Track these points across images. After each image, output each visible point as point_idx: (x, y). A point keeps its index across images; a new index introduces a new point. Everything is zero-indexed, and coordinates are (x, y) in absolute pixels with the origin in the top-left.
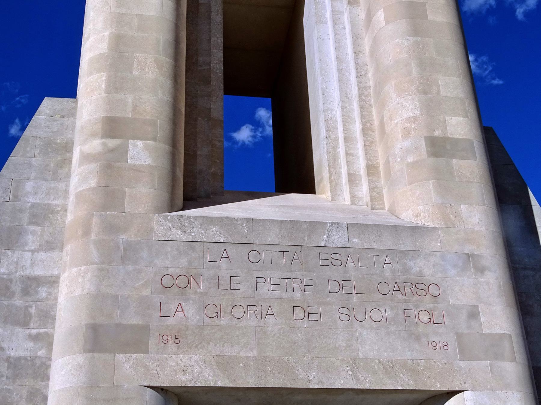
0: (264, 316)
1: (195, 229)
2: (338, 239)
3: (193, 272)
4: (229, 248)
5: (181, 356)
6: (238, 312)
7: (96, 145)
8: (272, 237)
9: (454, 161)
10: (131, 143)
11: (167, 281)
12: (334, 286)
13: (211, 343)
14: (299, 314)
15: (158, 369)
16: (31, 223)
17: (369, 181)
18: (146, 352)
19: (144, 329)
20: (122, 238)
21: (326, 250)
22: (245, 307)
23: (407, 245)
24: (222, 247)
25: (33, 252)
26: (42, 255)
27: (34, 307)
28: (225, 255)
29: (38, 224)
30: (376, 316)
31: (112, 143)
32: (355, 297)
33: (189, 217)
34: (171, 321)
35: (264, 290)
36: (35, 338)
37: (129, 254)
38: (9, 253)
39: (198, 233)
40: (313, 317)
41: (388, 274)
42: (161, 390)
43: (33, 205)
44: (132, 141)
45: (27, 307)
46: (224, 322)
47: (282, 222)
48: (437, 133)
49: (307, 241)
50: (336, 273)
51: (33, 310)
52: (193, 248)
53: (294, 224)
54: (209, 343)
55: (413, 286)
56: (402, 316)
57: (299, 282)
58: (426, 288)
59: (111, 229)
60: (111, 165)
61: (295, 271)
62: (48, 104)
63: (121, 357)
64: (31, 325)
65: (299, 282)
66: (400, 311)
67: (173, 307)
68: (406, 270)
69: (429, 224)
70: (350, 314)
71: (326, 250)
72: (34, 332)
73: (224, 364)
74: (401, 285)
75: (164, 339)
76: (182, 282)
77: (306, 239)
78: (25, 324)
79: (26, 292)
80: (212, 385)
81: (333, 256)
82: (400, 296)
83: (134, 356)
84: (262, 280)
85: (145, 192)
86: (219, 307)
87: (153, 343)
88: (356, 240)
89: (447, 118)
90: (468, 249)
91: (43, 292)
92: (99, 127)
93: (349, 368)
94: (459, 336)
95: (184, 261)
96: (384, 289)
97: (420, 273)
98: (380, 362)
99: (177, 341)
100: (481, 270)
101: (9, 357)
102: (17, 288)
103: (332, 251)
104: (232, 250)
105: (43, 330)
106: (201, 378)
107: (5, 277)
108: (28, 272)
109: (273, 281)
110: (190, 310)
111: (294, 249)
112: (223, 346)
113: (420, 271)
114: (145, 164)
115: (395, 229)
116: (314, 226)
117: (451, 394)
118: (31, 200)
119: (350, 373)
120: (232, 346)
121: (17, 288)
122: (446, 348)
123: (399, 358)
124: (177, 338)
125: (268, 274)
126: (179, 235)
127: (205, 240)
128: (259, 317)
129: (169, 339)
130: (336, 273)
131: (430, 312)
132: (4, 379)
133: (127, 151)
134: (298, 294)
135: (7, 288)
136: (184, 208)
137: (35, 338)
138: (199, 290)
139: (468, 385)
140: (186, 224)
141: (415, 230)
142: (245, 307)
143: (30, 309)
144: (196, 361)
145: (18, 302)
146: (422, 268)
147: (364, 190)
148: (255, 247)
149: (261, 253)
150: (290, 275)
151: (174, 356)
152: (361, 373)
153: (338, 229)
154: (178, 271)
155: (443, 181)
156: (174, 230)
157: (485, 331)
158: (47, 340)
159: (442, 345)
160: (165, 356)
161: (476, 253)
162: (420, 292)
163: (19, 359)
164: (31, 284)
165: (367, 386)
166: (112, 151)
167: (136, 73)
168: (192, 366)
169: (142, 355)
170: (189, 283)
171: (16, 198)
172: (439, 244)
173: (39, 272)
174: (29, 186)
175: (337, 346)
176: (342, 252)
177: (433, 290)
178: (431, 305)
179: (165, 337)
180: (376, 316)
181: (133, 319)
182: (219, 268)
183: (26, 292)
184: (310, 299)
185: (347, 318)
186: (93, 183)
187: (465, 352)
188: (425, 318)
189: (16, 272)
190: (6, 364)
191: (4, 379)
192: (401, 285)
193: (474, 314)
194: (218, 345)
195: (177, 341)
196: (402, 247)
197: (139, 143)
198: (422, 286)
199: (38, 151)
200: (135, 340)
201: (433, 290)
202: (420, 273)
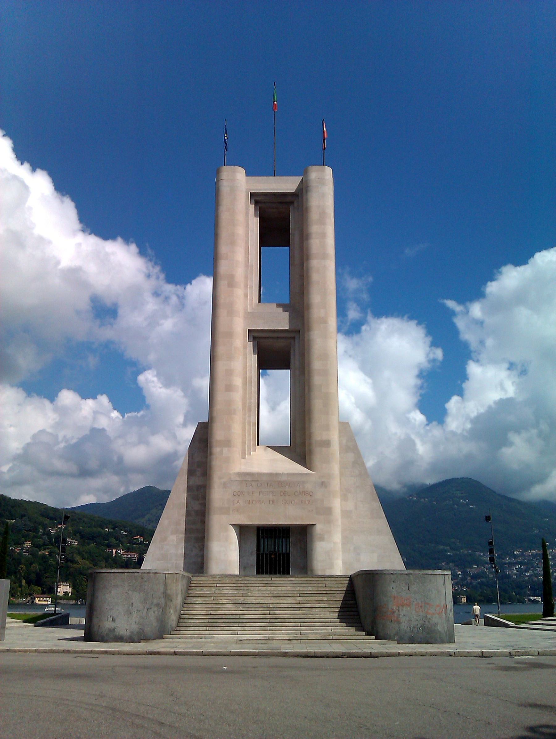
2: (284, 478)
12: (282, 494)
35: (261, 495)
46: (250, 505)
55: (304, 493)
76: (239, 493)
79: (197, 490)
82: (300, 496)
90: (323, 480)
104: (253, 483)
116: (277, 474)
124: (237, 510)
126: (238, 479)
134: (271, 496)
146: (309, 487)
177: (311, 494)
181: (226, 506)
188: (307, 502)
200: (225, 511)
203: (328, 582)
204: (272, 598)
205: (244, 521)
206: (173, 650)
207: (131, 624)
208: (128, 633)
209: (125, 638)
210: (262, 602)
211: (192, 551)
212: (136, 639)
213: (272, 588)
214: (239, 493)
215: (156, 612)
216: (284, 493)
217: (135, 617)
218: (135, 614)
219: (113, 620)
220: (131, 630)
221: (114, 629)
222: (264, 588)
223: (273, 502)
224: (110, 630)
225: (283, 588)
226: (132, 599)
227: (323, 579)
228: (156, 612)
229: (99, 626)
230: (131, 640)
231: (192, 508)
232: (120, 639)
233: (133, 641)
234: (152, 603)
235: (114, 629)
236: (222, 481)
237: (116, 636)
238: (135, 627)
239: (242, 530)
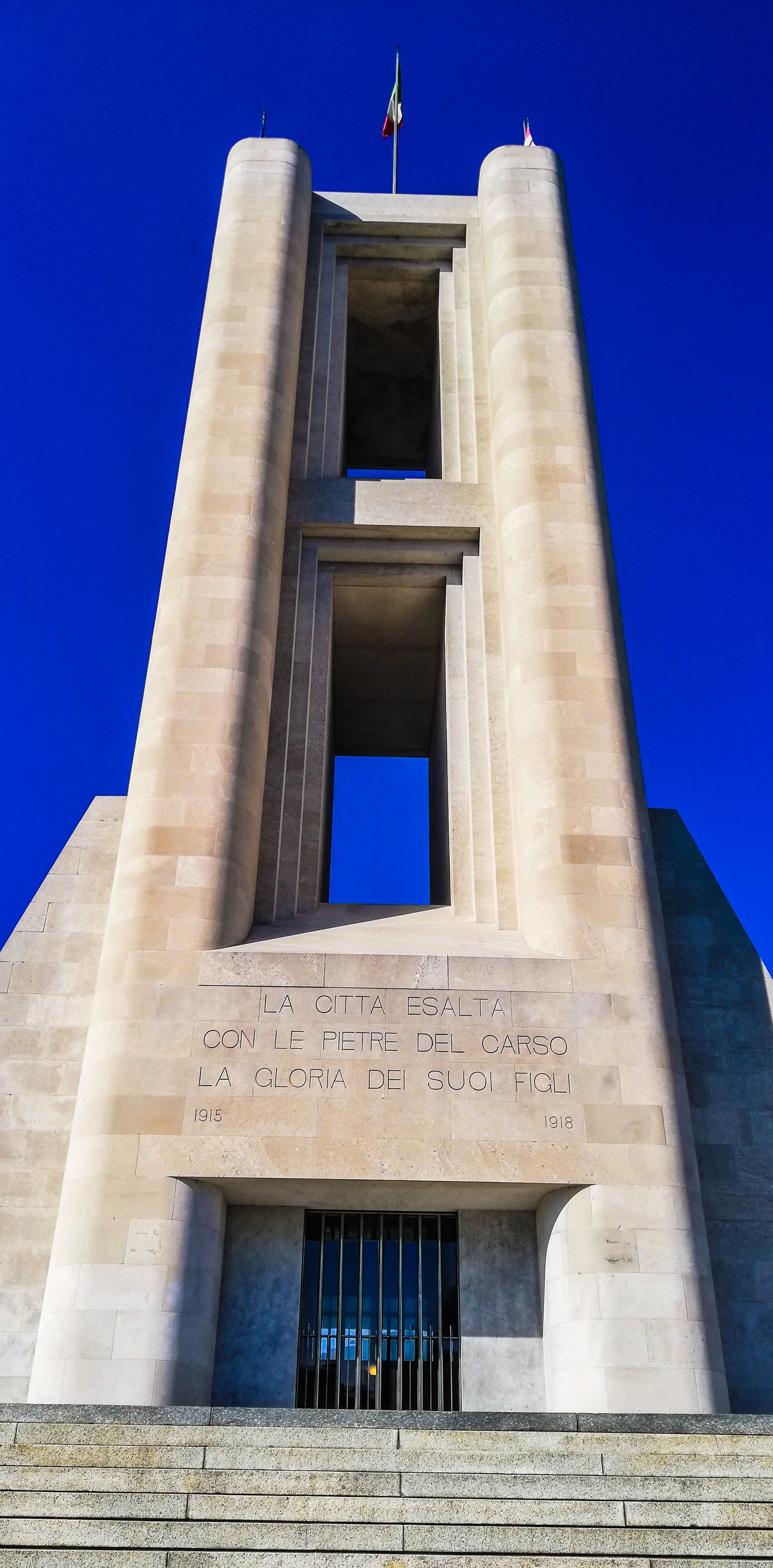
0: (330, 1084)
1: (251, 970)
2: (434, 979)
3: (244, 1027)
4: (292, 993)
5: (222, 1138)
8: (349, 978)
9: (599, 867)
10: (181, 858)
11: (212, 1039)
12: (425, 1042)
13: (260, 1120)
15: (192, 1155)
17: (499, 891)
18: (179, 1133)
21: (418, 993)
22: (308, 1073)
23: (526, 983)
24: (284, 992)
27: (64, 1067)
28: (287, 1003)
29: (76, 961)
30: (478, 1081)
31: (158, 860)
32: (452, 1057)
33: (245, 954)
34: (213, 1092)
38: (39, 997)
39: (256, 974)
40: (393, 1084)
42: (193, 1182)
44: (182, 857)
45: (56, 1067)
46: (278, 1092)
48: (577, 831)
49: (393, 982)
50: (430, 1026)
51: (61, 1072)
52: (248, 995)
54: (258, 1120)
55: (529, 1041)
56: (513, 1082)
57: (379, 1037)
58: (548, 1043)
59: (147, 972)
61: (375, 1023)
62: (100, 805)
63: (146, 1139)
64: (59, 1091)
65: (379, 1037)
66: (511, 1075)
67: (217, 1073)
69: (559, 955)
70: (443, 1081)
71: (418, 993)
72: (62, 1099)
73: (275, 1148)
74: (514, 1040)
75: (201, 1115)
76: (230, 1039)
77: (392, 979)
80: (258, 1176)
81: (424, 1001)
83: (163, 1137)
84: (332, 1036)
86: (274, 1072)
87: (188, 1118)
88: (458, 979)
89: (592, 809)
93: (436, 1154)
94: (588, 1109)
95: (234, 1013)
96: (491, 1044)
97: (541, 1023)
98: (478, 1145)
99: (218, 1118)
100: (625, 1017)
101: (30, 1132)
102: (44, 1043)
103: (425, 994)
105: (72, 1098)
106: (244, 1167)
107: (32, 1029)
109: (346, 1037)
110: (238, 1077)
111: (376, 993)
112: (276, 1124)
113: (541, 1020)
114: (195, 886)
115: (512, 963)
116: (404, 961)
117: (573, 1189)
119: (438, 1159)
120: (287, 1124)
122: (569, 1125)
123: (504, 1139)
124: (216, 1114)
125: (339, 1027)
126: (231, 977)
127: (263, 984)
128: (324, 1085)
129: (209, 1115)
130: (430, 1026)
131: (552, 1077)
132: (22, 1160)
133: (175, 871)
134: (376, 1053)
135: (34, 1043)
136: (248, 939)
138: (251, 1050)
139: (595, 1176)
140: (241, 964)
141: (538, 964)
142: (308, 1073)
143: (59, 1070)
144: (240, 1145)
145: (45, 1062)
147: (493, 904)
148: (326, 992)
149: (333, 1000)
150: (367, 1028)
151: (212, 1137)
152: (451, 1160)
153: (436, 965)
154: (227, 1026)
155: (582, 895)
156: (225, 971)
157: (626, 1101)
159: (564, 1122)
160: (202, 1137)
161: (619, 993)
162: (539, 1049)
165: (459, 1178)
166: (157, 871)
167: (193, 768)
168: (235, 1150)
169: (174, 1136)
170: (239, 1041)
172: (570, 983)
173: (72, 1022)
174: (68, 911)
175: (423, 1123)
176: (439, 995)
178: (553, 1067)
179: (204, 1113)
180: (478, 1081)
181: (165, 1089)
182: (278, 1020)
183: (56, 1048)
184: (392, 1060)
185: (438, 1085)
187: (593, 1133)
189: (45, 1022)
190: (26, 1141)
191: (22, 1160)
192: (514, 1040)
193: (609, 1080)
194: (269, 1123)
195: (218, 1118)
196: (520, 988)
197: (191, 859)
198: (542, 1041)
199: (82, 865)
200: (164, 1117)
202: (541, 1023)
213: (413, 1511)
214: (230, 1039)
222: (348, 1509)
223: (387, 1078)
225: (500, 1513)
231: (22, 1122)
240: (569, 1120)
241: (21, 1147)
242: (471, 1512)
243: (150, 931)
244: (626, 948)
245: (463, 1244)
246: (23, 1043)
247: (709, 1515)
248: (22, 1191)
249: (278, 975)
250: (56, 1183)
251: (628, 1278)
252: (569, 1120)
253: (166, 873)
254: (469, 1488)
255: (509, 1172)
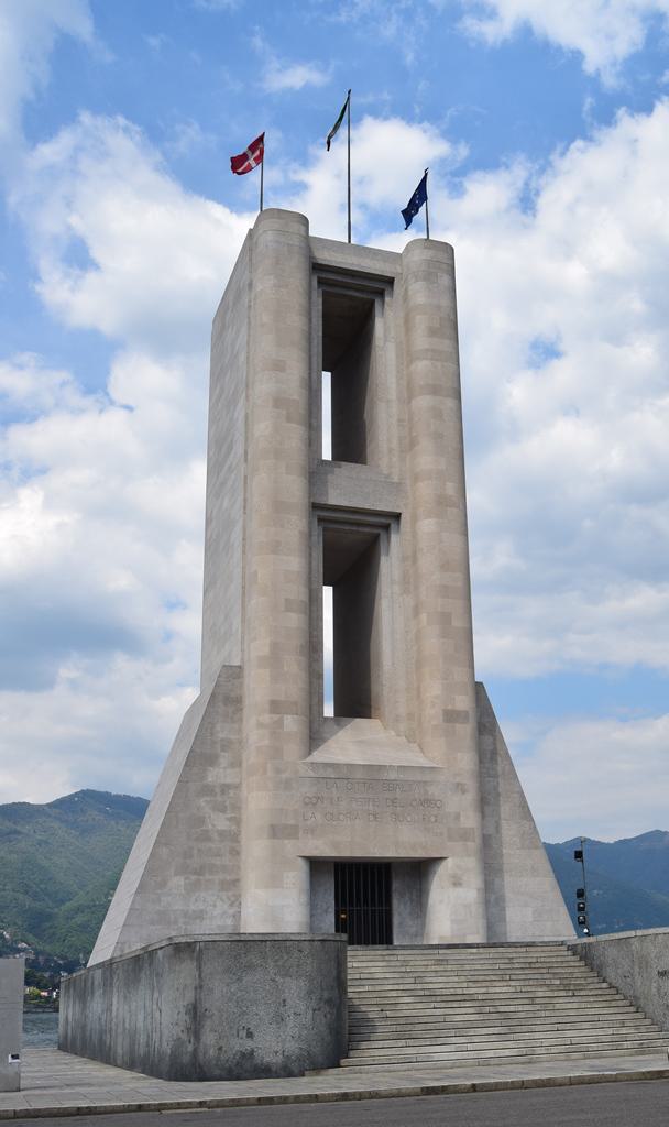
2: (393, 776)
6: (341, 817)
7: (267, 718)
8: (359, 775)
10: (285, 716)
11: (307, 800)
14: (371, 818)
16: (223, 750)
19: (296, 827)
20: (284, 776)
24: (333, 781)
25: (225, 768)
26: (228, 771)
31: (276, 717)
34: (309, 823)
36: (230, 819)
37: (287, 785)
41: (416, 796)
43: (222, 740)
47: (364, 765)
48: (450, 707)
51: (227, 803)
53: (370, 767)
55: (427, 802)
59: (278, 771)
60: (276, 730)
63: (286, 841)
68: (426, 792)
78: (223, 810)
79: (223, 792)
81: (390, 785)
85: (293, 750)
87: (301, 833)
90: (458, 780)
91: (232, 793)
92: (267, 707)
96: (414, 803)
100: (464, 792)
102: (218, 790)
108: (223, 781)
110: (318, 816)
115: (422, 769)
116: (381, 768)
118: (221, 736)
121: (218, 790)
124: (312, 831)
126: (312, 774)
131: (436, 816)
134: (371, 807)
137: (230, 819)
145: (219, 798)
146: (434, 791)
157: (462, 826)
158: (237, 821)
163: (224, 831)
164: (225, 788)
167: (285, 669)
171: (212, 734)
173: (228, 781)
174: (218, 727)
181: (292, 822)
183: (223, 792)
186: (267, 742)
188: (433, 819)
193: (457, 817)
197: (289, 717)
200: (291, 832)
201: (438, 804)
203: (534, 954)
204: (471, 984)
205: (324, 848)
206: (469, 1083)
207: (284, 1041)
208: (279, 1059)
209: (274, 1069)
210: (459, 991)
211: (215, 906)
212: (296, 1071)
214: (314, 800)
215: (329, 1016)
216: (394, 801)
217: (292, 1027)
218: (291, 1021)
219: (250, 1035)
220: (286, 1054)
221: (253, 1051)
223: (375, 816)
224: (243, 1055)
226: (284, 992)
227: (524, 949)
228: (329, 1016)
229: (220, 1049)
230: (287, 1072)
231: (214, 826)
232: (265, 1072)
233: (290, 1074)
234: (321, 999)
235: (253, 1051)
236: (284, 776)
237: (256, 1065)
238: (292, 1047)
239: (316, 865)
240: (441, 834)
241: (216, 836)
242: (467, 967)
243: (276, 752)
244: (466, 761)
245: (393, 875)
246: (207, 790)
247: (517, 966)
248: (218, 855)
249: (331, 773)
250: (235, 853)
251: (460, 891)
252: (441, 834)
253: (280, 723)
254: (466, 962)
255: (419, 854)
